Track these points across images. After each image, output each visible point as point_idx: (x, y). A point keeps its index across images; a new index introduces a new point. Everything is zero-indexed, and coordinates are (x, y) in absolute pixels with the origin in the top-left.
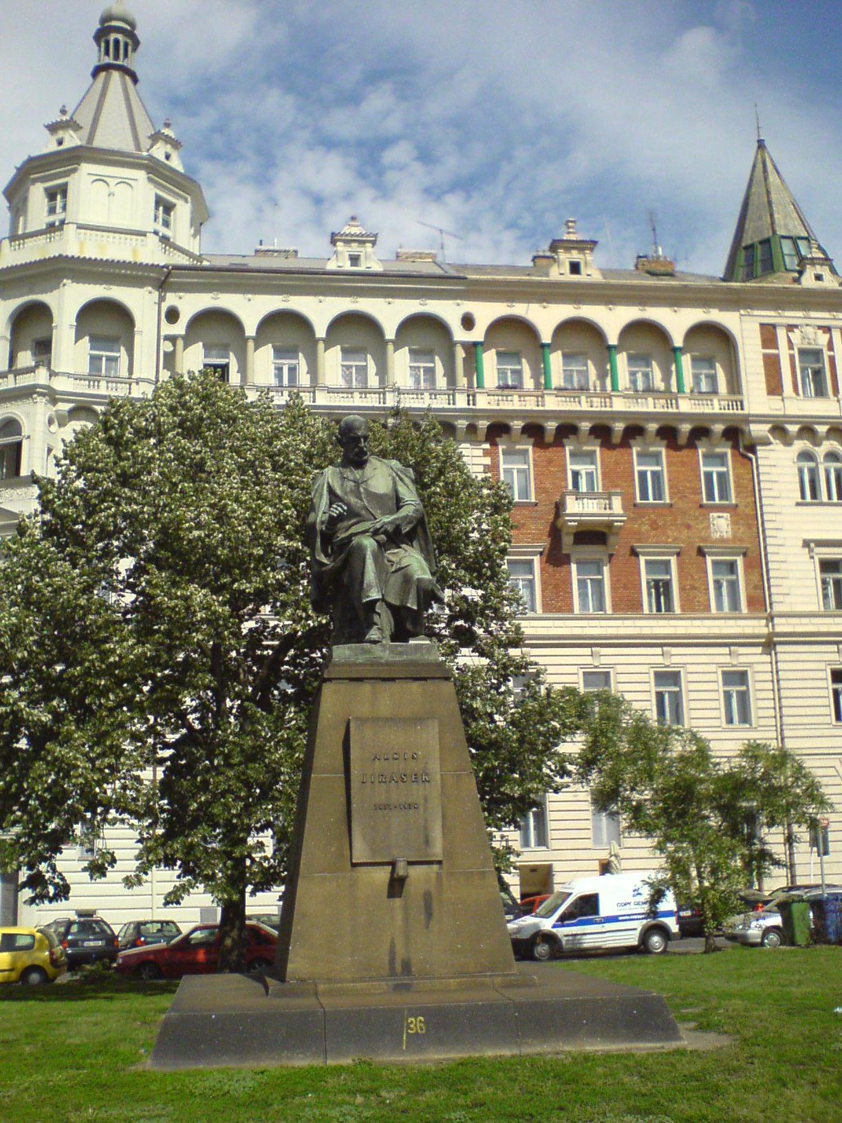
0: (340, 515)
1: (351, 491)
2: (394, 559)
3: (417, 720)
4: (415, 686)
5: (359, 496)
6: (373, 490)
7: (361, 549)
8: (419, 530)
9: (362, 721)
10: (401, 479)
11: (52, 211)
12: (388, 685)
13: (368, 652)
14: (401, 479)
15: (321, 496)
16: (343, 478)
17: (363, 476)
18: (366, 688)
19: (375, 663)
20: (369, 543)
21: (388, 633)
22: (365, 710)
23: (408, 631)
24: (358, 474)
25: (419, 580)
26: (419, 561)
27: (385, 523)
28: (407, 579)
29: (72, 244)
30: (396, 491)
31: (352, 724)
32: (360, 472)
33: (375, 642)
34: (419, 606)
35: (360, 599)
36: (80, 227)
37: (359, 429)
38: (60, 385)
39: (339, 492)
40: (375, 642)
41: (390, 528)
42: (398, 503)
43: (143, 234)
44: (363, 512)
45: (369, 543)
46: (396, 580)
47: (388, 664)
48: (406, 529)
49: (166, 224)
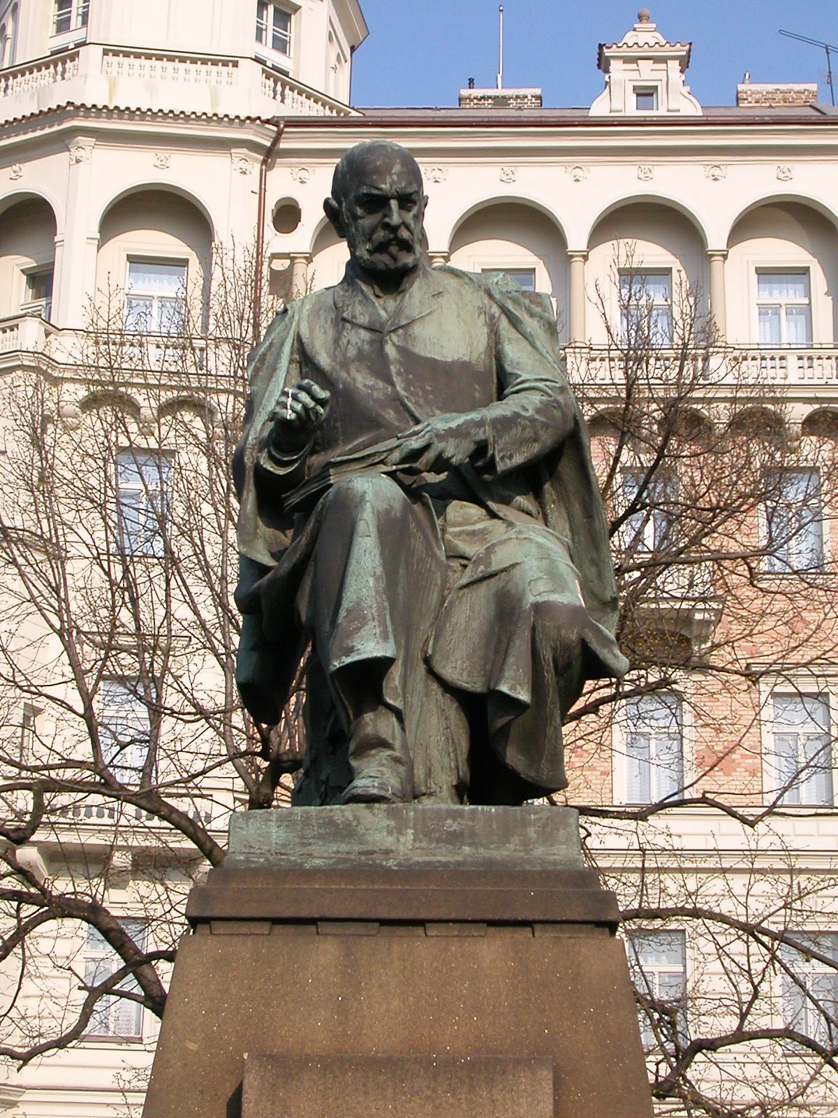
0: (306, 417)
1: (361, 356)
2: (470, 549)
3: (484, 1067)
4: (491, 951)
5: (377, 364)
6: (425, 349)
7: (347, 507)
8: (566, 467)
9: (286, 1066)
10: (515, 322)
11: (63, 25)
12: (399, 945)
13: (346, 832)
14: (515, 322)
15: (274, 369)
16: (341, 321)
17: (398, 312)
18: (325, 952)
19: (367, 870)
20: (374, 491)
21: (445, 780)
22: (313, 1029)
23: (513, 774)
24: (384, 307)
25: (537, 607)
26: (545, 555)
27: (441, 437)
28: (506, 610)
29: (91, 83)
30: (498, 356)
31: (252, 1082)
32: (391, 303)
33: (370, 800)
34: (537, 688)
35: (329, 664)
36: (110, 51)
37: (385, 171)
38: (67, 350)
39: (324, 360)
40: (370, 800)
41: (457, 452)
42: (502, 383)
43: (231, 62)
44: (390, 415)
45: (374, 491)
46: (470, 614)
47: (410, 873)
48: (510, 458)
49: (281, 45)
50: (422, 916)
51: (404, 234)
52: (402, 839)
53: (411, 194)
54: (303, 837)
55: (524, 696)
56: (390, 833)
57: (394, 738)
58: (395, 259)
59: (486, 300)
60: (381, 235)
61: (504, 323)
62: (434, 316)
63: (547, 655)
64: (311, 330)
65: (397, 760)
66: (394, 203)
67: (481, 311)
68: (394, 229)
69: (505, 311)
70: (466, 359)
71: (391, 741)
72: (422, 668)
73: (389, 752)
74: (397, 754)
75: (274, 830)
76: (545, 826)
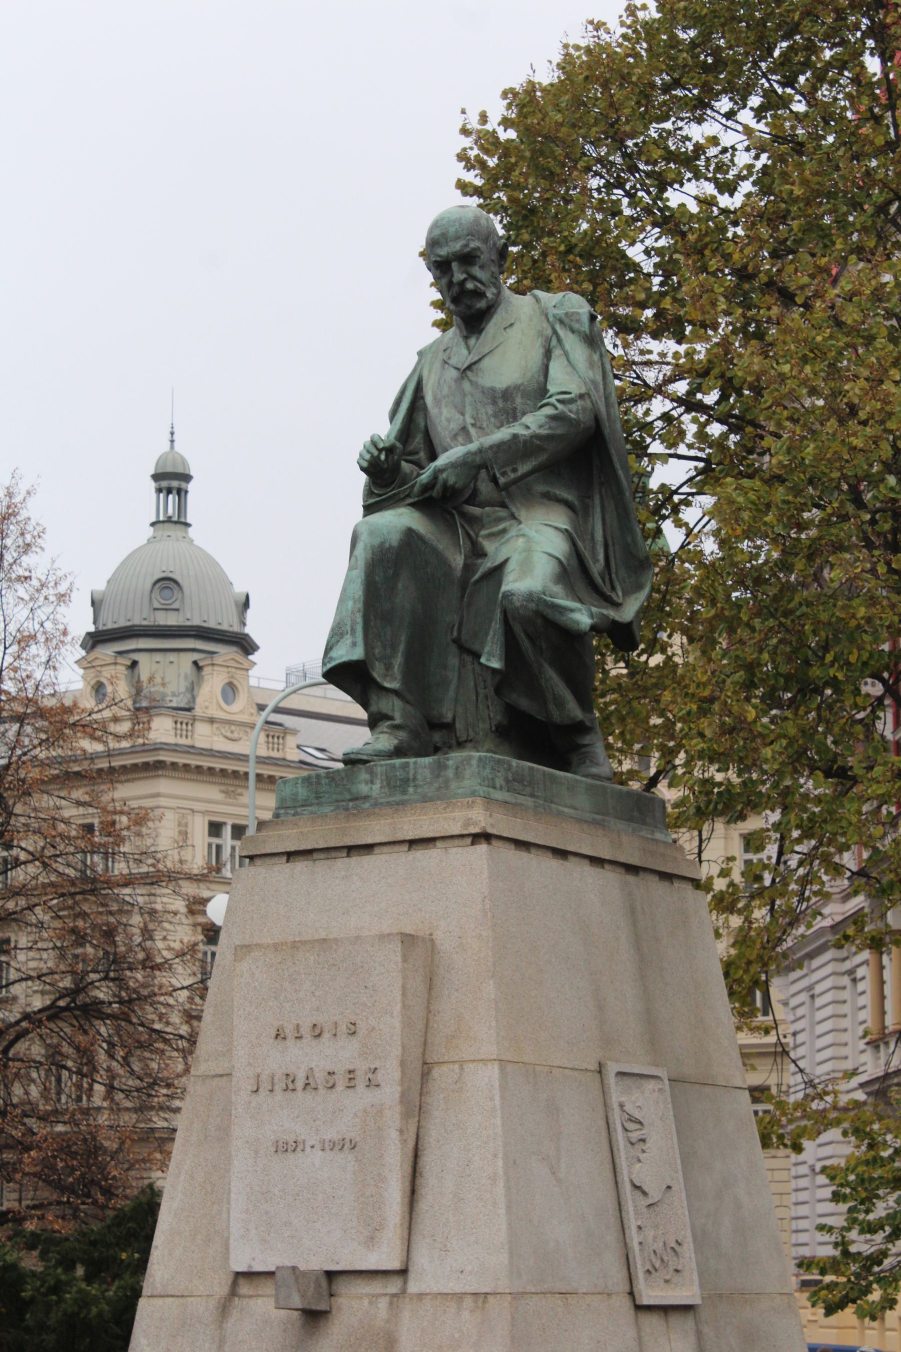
14: (559, 340)
50: (370, 841)
51: (470, 285)
52: (374, 787)
53: (469, 253)
54: (317, 793)
55: (496, 664)
56: (367, 783)
57: (393, 710)
58: (469, 307)
59: (545, 324)
60: (456, 289)
61: (554, 342)
62: (501, 348)
63: (517, 629)
64: (430, 371)
65: (397, 727)
66: (455, 265)
67: (540, 334)
68: (462, 283)
69: (555, 332)
70: (519, 382)
71: (390, 714)
72: (454, 649)
73: (389, 723)
74: (398, 721)
75: (300, 790)
76: (457, 768)
